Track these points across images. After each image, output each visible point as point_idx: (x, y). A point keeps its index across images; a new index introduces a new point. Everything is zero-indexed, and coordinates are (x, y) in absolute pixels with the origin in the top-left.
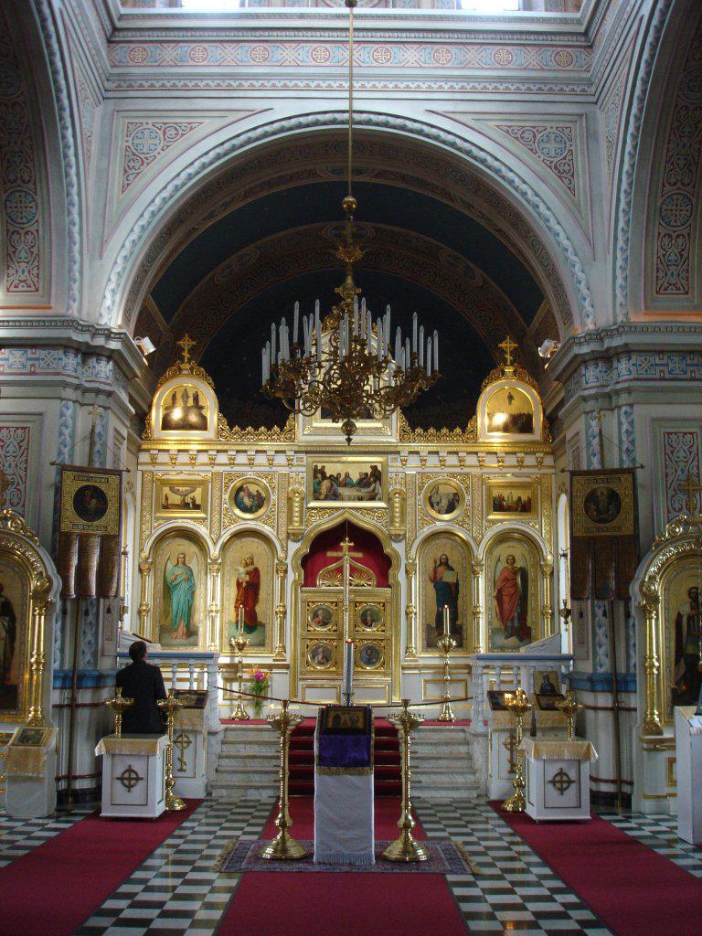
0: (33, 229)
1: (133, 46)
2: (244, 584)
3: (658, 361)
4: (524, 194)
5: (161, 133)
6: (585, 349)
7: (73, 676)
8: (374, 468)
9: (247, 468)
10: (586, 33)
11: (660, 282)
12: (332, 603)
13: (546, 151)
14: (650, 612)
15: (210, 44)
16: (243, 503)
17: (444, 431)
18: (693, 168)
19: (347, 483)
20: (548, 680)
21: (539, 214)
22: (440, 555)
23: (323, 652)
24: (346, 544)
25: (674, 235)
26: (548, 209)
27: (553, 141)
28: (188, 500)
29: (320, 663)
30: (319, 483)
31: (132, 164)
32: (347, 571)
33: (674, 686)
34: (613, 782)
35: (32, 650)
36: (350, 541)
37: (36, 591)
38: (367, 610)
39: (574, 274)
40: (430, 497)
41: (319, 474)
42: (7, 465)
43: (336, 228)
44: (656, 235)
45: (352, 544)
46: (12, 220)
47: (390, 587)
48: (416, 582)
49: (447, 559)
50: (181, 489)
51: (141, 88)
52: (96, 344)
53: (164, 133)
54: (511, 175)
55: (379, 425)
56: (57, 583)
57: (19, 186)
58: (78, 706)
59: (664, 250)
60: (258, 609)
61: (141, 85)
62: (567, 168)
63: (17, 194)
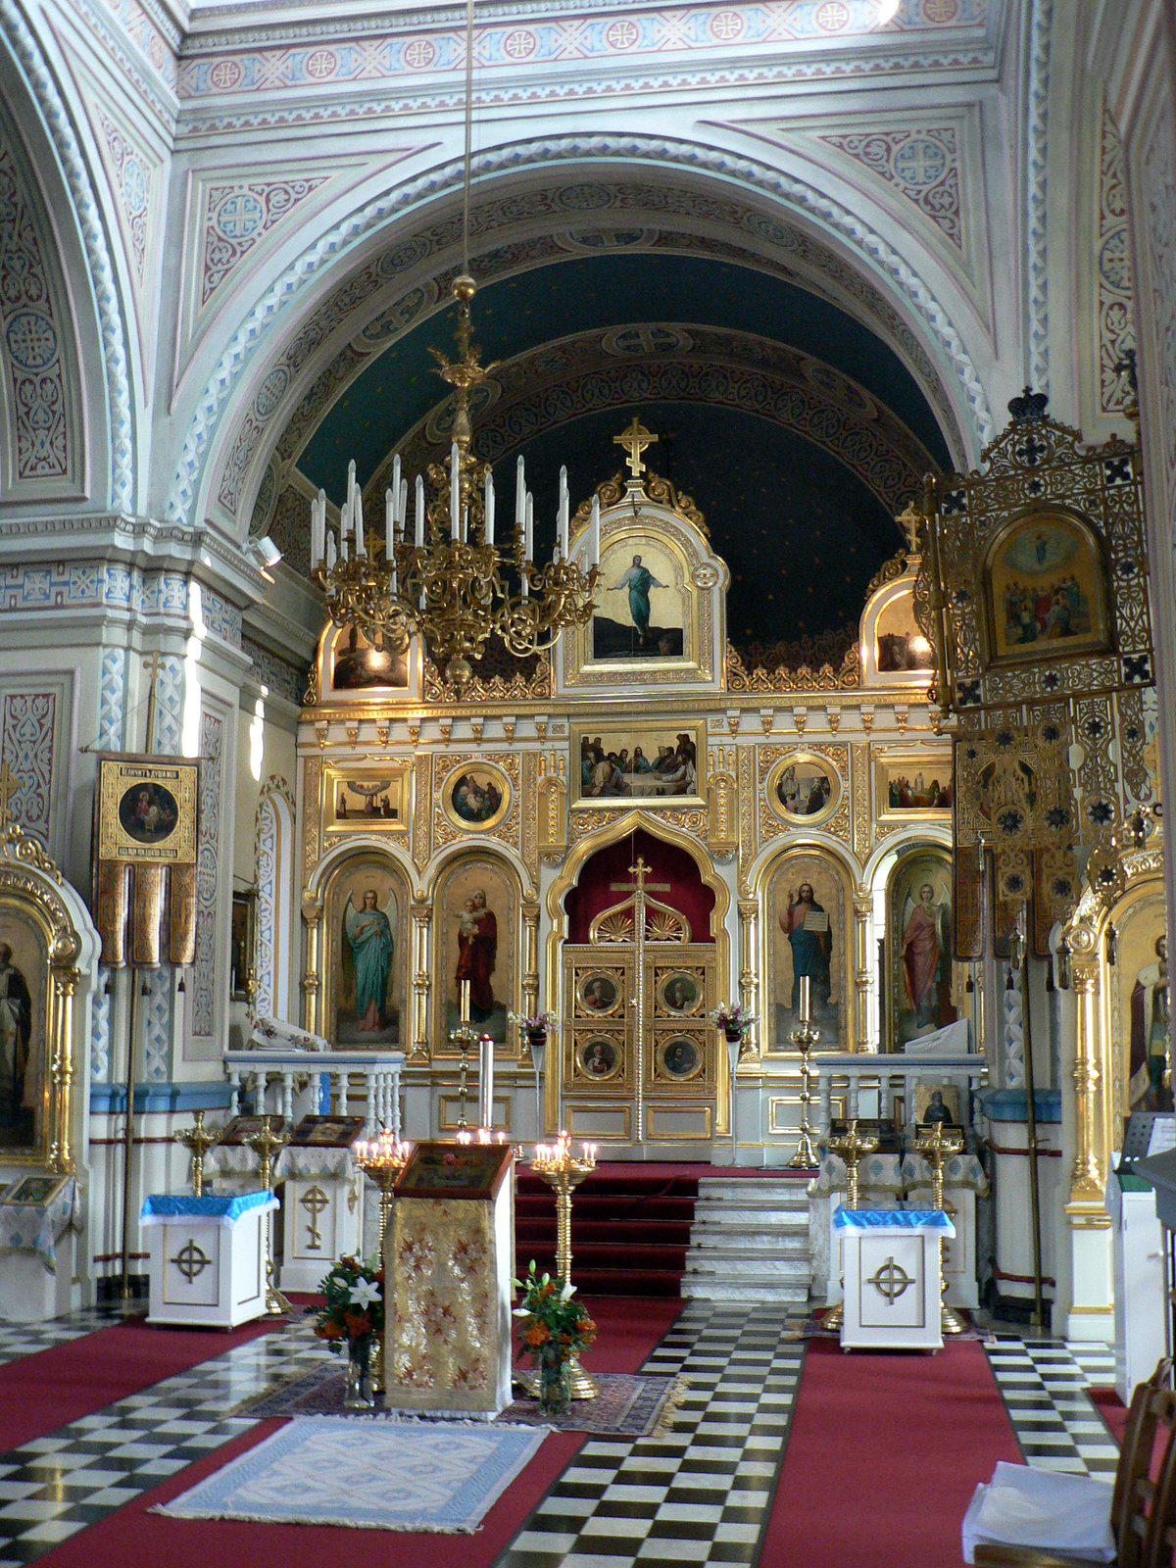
0: (53, 373)
1: (216, 60)
2: (471, 941)
4: (873, 252)
5: (262, 200)
7: (128, 1094)
8: (684, 739)
9: (473, 747)
11: (1108, 391)
12: (617, 969)
13: (908, 174)
14: (1083, 982)
15: (339, 46)
16: (466, 804)
17: (804, 670)
19: (639, 766)
20: (940, 1101)
21: (901, 284)
22: (799, 884)
23: (602, 1052)
24: (640, 869)
26: (915, 274)
27: (921, 156)
28: (378, 803)
29: (597, 1071)
30: (591, 768)
31: (217, 256)
32: (641, 916)
33: (1128, 1114)
34: (1029, 1280)
35: (55, 1052)
37: (57, 959)
38: (676, 981)
39: (963, 384)
40: (780, 786)
41: (590, 751)
42: (21, 755)
43: (624, 336)
44: (1096, 305)
45: (649, 870)
46: (21, 362)
47: (713, 940)
48: (758, 933)
49: (811, 891)
50: (365, 784)
52: (161, 553)
53: (268, 200)
54: (848, 220)
55: (692, 665)
56: (91, 944)
57: (25, 306)
58: (138, 1141)
59: (1112, 331)
60: (493, 981)
61: (230, 125)
62: (946, 200)
63: (24, 320)
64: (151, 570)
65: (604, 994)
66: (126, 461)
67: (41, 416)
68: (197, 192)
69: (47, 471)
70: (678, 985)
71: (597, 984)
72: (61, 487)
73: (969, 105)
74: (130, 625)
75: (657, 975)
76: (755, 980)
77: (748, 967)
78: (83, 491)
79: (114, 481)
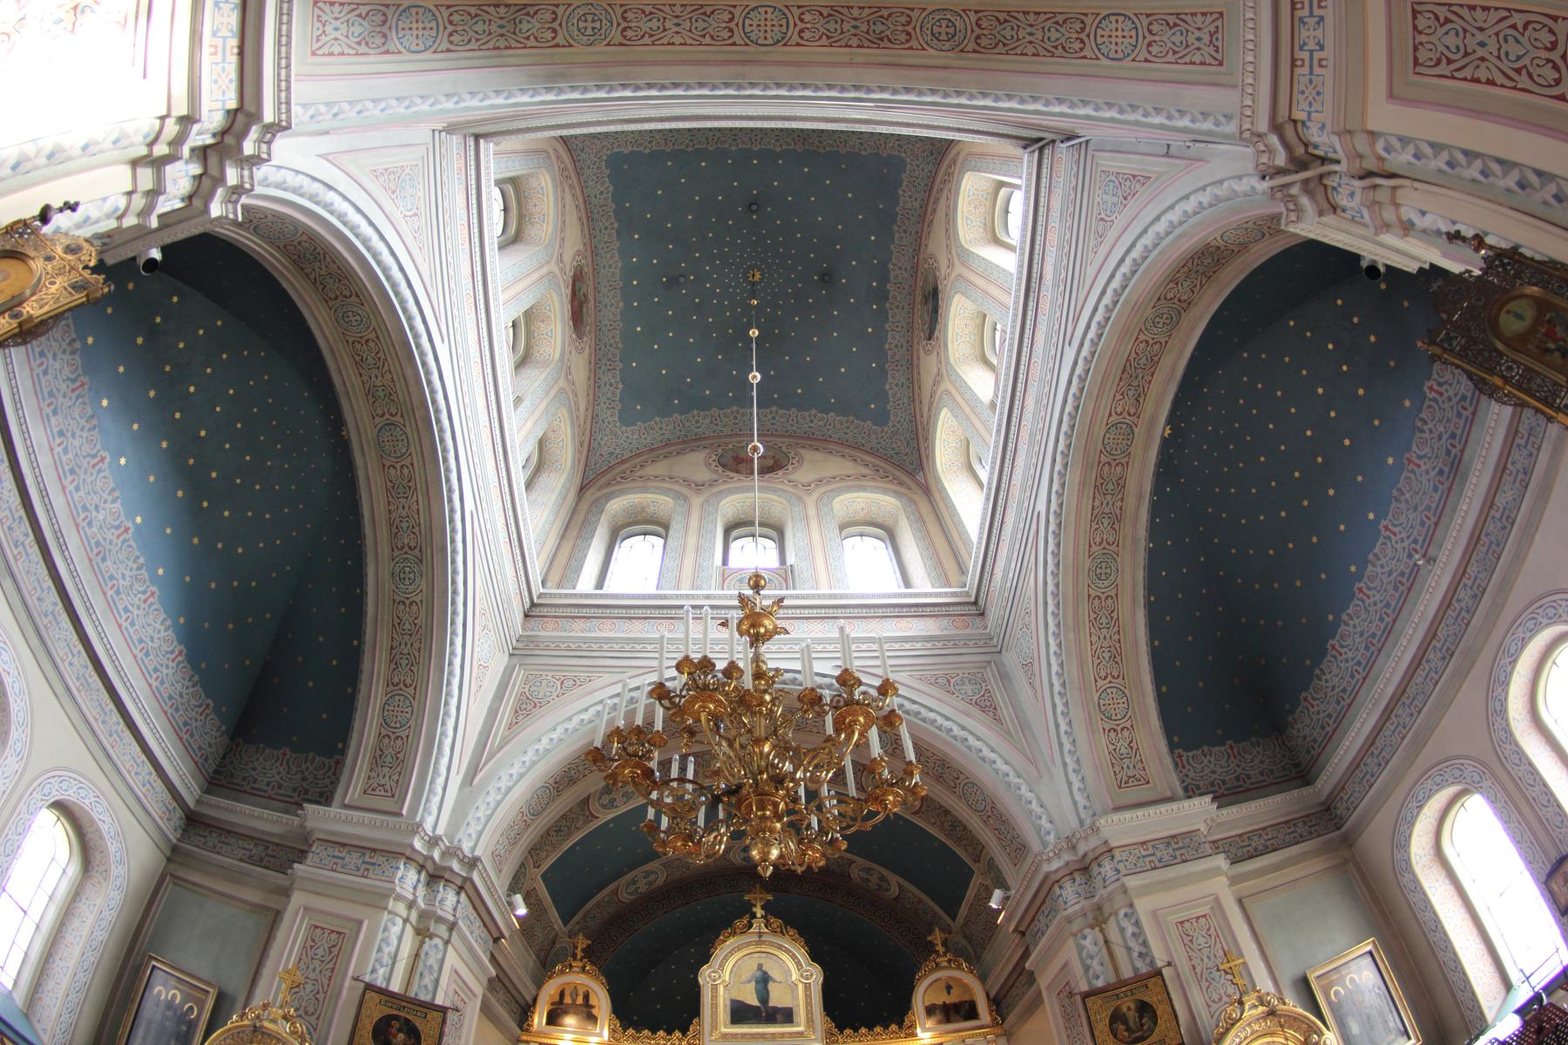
0: (403, 734)
3: (1144, 853)
5: (559, 683)
6: (1055, 865)
10: (975, 603)
11: (1119, 777)
18: (1118, 659)
25: (1119, 729)
39: (1020, 797)
51: (547, 648)
54: (932, 715)
63: (397, 698)
64: (435, 877)
66: (436, 800)
67: (389, 759)
68: (519, 675)
69: (382, 793)
72: (387, 804)
73: (989, 662)
74: (411, 905)
78: (402, 808)
79: (424, 810)
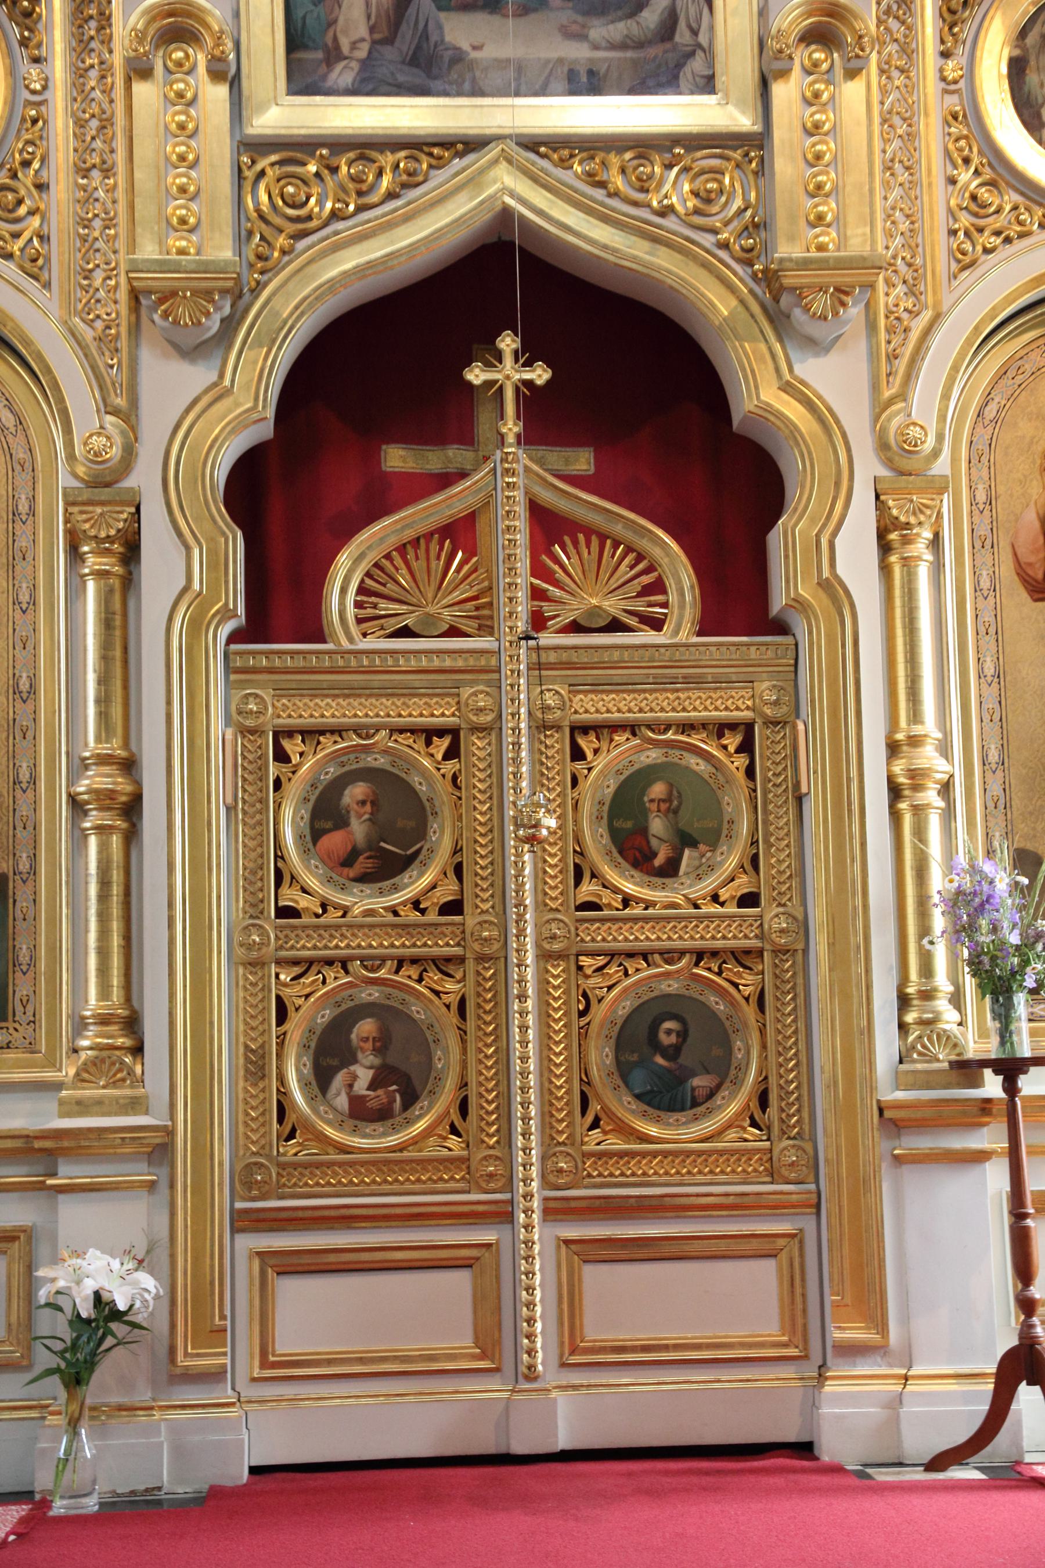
12: (430, 734)
23: (382, 1044)
36: (528, 356)
38: (641, 778)
45: (540, 374)
47: (780, 628)
65: (380, 829)
70: (658, 790)
71: (357, 791)
75: (577, 754)
76: (940, 767)
77: (916, 717)
